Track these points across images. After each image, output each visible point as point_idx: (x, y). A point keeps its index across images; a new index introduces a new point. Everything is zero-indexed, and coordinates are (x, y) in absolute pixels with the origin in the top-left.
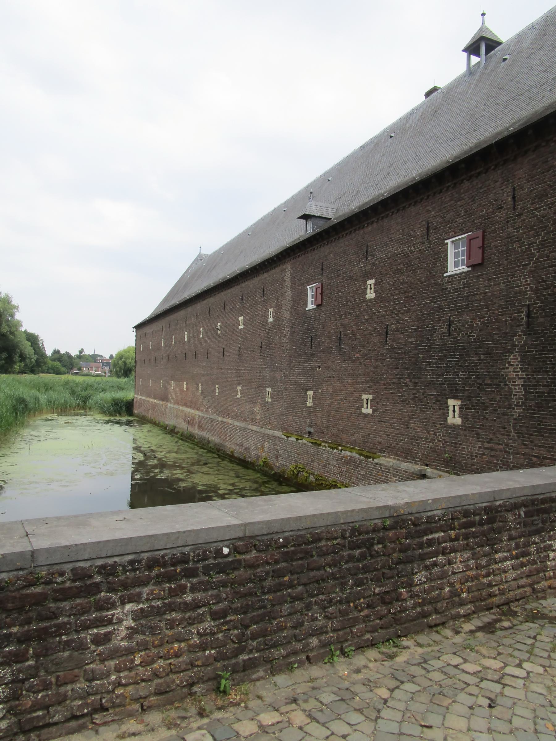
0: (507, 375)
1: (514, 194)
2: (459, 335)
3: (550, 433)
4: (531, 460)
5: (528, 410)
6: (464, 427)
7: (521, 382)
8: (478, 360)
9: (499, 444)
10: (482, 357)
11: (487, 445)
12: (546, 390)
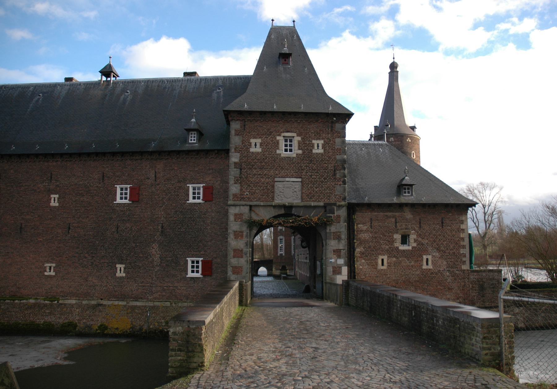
0: (151, 253)
1: (156, 175)
2: (123, 233)
3: (173, 276)
4: (163, 288)
5: (162, 267)
6: (127, 277)
7: (159, 256)
8: (135, 246)
9: (148, 283)
10: (138, 244)
11: (140, 285)
12: (170, 259)
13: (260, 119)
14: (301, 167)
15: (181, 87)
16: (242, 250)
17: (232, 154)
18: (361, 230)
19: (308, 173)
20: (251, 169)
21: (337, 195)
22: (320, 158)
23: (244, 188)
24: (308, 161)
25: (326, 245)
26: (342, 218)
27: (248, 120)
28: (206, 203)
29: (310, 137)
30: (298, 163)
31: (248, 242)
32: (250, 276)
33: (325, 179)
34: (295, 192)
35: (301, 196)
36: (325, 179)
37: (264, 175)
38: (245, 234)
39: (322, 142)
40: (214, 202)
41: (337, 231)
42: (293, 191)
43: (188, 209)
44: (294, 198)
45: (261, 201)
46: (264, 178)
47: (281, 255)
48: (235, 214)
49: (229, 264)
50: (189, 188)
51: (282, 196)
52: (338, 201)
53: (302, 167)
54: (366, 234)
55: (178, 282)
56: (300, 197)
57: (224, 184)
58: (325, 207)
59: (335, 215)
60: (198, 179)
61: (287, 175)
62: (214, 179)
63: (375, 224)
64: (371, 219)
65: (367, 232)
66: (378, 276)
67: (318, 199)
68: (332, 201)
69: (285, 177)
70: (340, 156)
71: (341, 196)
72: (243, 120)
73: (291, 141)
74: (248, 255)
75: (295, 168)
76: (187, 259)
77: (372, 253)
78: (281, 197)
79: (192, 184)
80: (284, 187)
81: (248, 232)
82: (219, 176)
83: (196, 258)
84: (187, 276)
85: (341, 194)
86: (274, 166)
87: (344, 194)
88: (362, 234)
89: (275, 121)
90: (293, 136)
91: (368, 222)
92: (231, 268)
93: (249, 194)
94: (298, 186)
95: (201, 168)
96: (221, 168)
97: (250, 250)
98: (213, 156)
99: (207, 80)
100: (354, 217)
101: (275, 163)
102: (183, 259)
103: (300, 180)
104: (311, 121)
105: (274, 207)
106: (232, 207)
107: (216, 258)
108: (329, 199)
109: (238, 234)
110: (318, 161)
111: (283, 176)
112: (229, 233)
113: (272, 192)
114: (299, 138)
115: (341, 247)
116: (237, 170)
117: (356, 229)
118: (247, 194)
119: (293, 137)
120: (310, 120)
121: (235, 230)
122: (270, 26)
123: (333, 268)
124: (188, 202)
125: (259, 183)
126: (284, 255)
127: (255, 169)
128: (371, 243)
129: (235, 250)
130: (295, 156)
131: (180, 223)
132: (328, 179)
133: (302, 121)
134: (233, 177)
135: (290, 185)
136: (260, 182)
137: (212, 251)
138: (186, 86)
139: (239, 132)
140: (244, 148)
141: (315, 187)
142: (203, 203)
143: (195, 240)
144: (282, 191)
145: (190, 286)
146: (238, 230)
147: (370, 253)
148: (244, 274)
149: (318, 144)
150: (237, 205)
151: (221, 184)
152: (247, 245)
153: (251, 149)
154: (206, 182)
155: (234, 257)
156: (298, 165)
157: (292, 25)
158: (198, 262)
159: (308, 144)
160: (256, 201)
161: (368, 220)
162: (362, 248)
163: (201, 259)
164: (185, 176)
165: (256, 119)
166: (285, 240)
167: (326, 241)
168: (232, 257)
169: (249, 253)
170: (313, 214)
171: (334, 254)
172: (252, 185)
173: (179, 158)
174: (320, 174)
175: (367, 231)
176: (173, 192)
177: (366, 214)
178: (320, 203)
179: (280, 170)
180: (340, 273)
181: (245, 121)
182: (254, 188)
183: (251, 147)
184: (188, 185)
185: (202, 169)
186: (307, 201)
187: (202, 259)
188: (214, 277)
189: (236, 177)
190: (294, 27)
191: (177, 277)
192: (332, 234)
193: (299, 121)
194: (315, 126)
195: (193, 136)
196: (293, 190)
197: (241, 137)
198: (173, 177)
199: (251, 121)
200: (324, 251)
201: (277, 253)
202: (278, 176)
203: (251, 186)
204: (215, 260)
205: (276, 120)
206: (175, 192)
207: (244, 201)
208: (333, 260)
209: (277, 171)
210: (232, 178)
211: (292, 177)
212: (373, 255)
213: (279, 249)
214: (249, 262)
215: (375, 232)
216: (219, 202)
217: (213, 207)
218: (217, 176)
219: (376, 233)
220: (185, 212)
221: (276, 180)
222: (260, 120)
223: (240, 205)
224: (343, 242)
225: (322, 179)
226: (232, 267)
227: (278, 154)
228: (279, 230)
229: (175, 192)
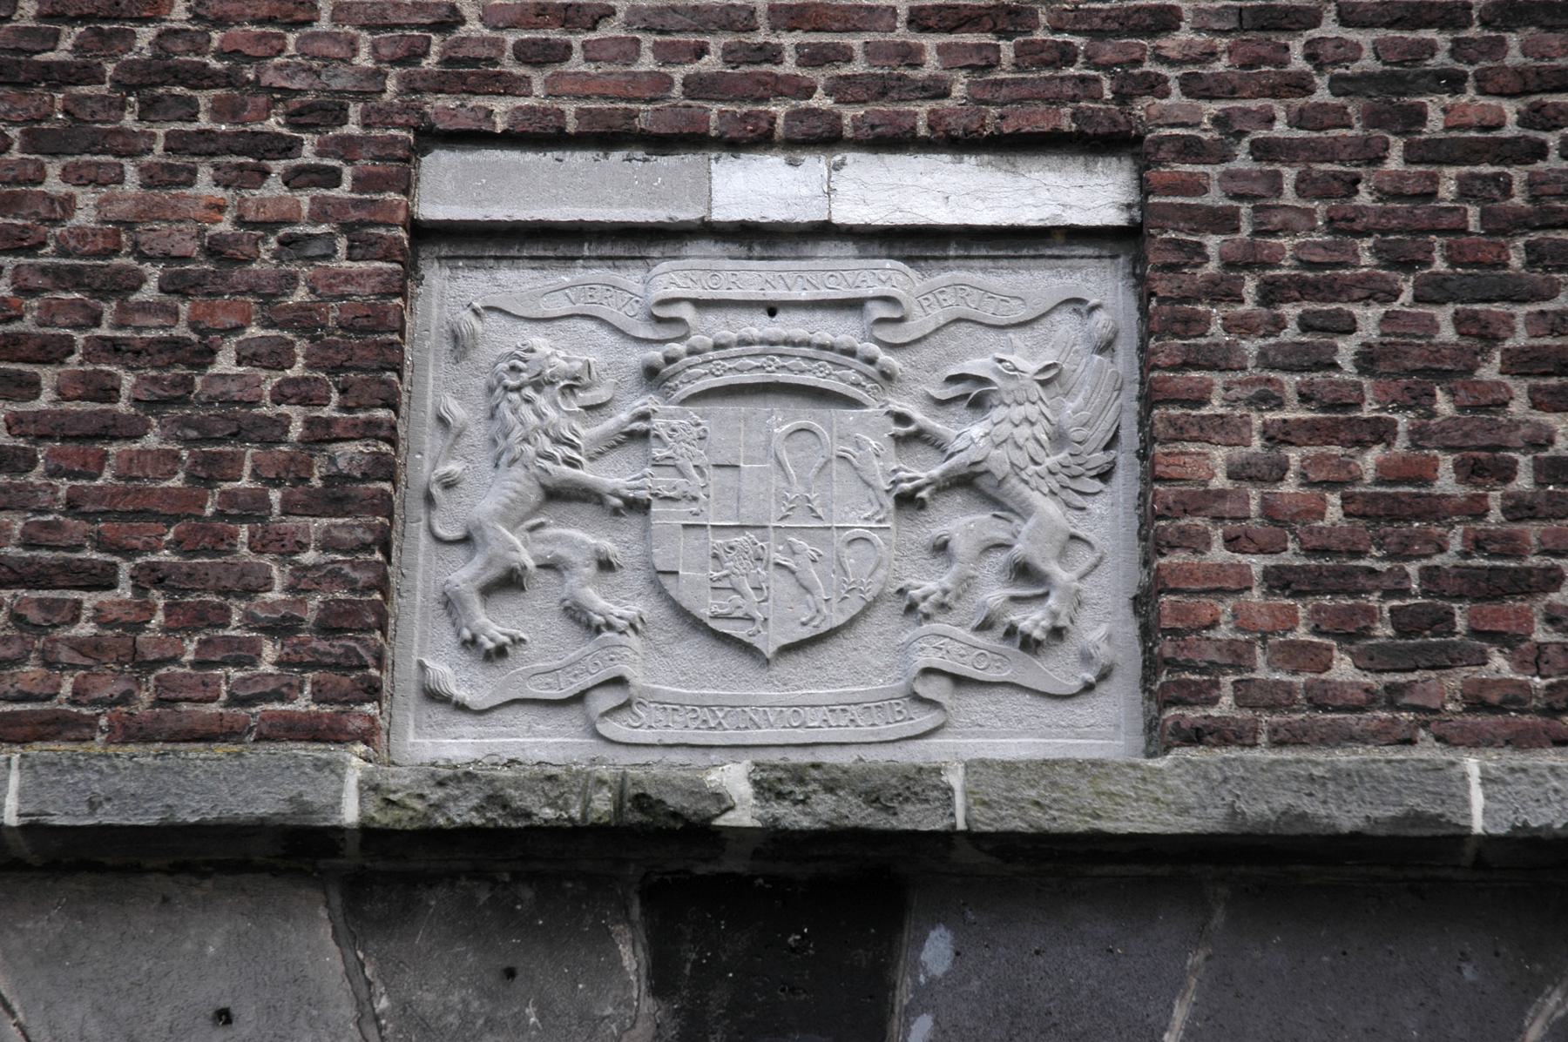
35: (1142, 602)
42: (924, 469)
46: (130, 147)
51: (599, 600)
69: (692, 140)
78: (579, 617)
80: (652, 376)
111: (646, 116)
113: (336, 497)
141: (1518, 364)
144: (614, 476)
196: (912, 438)
202: (502, 111)
221: (431, 209)
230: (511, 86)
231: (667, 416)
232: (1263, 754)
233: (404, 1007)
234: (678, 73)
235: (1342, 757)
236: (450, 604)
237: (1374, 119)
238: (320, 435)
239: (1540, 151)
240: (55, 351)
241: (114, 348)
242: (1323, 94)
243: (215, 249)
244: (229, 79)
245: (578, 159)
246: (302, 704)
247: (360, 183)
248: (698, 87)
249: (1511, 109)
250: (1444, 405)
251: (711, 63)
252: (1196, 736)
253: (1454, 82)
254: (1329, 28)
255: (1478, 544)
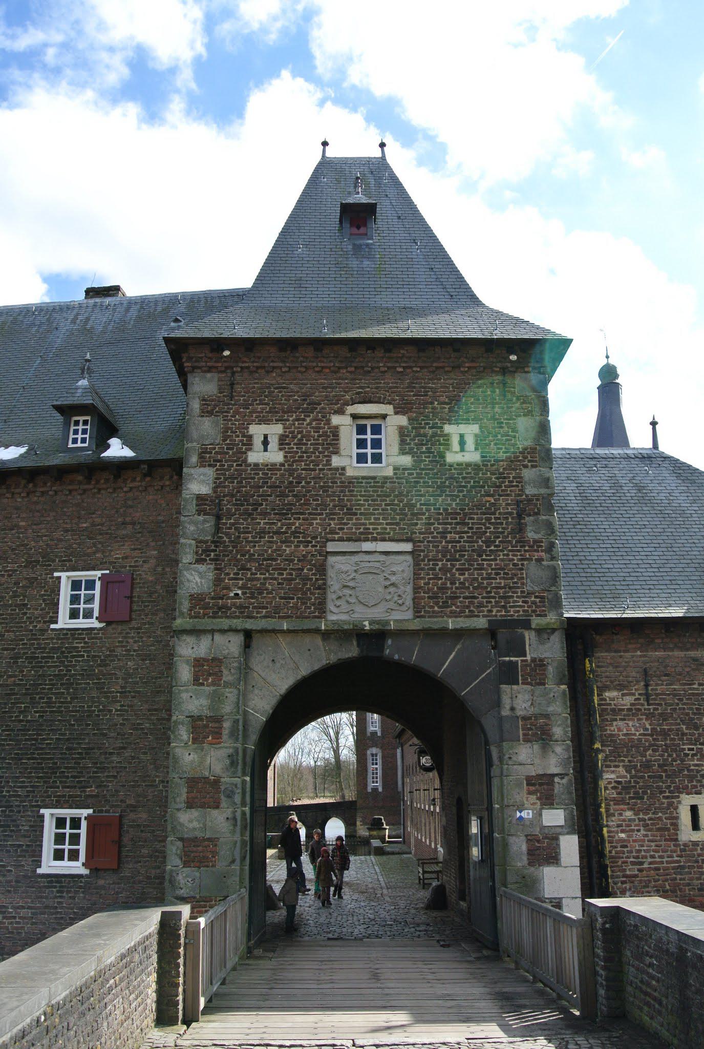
13: (281, 364)
14: (411, 506)
15: (74, 321)
16: (217, 782)
17: (192, 471)
18: (613, 710)
19: (433, 524)
20: (250, 514)
21: (530, 594)
22: (472, 478)
23: (228, 574)
24: (431, 489)
25: (501, 759)
26: (550, 668)
27: (242, 368)
28: (110, 628)
29: (435, 415)
30: (401, 494)
31: (237, 753)
32: (242, 870)
33: (488, 543)
34: (393, 584)
35: (414, 599)
36: (488, 543)
37: (293, 533)
38: (227, 725)
39: (475, 428)
40: (134, 624)
41: (536, 710)
42: (388, 583)
43: (53, 648)
44: (391, 605)
45: (283, 617)
46: (293, 542)
47: (375, 790)
48: (195, 659)
49: (174, 828)
50: (60, 582)
51: (350, 600)
52: (534, 611)
53: (414, 505)
54: (631, 723)
55: (9, 891)
56: (409, 602)
57: (168, 569)
58: (492, 632)
59: (528, 658)
60: (88, 555)
61: (367, 532)
62: (136, 554)
63: (660, 687)
64: (645, 671)
65: (633, 715)
66: (682, 867)
67: (468, 607)
68: (515, 613)
70: (534, 469)
71: (543, 597)
72: (227, 368)
73: (377, 430)
74: (238, 799)
75: (391, 509)
76: (42, 811)
77: (658, 787)
78: (348, 602)
79: (67, 571)
81: (238, 720)
82: (153, 544)
83: (71, 807)
84: (39, 871)
85: (544, 591)
86: (324, 505)
87: (553, 588)
88: (620, 723)
89: (328, 370)
90: (383, 412)
91: (638, 682)
92: (180, 844)
93: (244, 593)
94: (403, 568)
95: (98, 520)
96: (161, 518)
97: (244, 782)
98: (137, 484)
99: (144, 302)
100: (588, 665)
101: (328, 496)
102: (29, 813)
103: (408, 547)
104: (437, 368)
105: (326, 635)
106: (185, 637)
107: (133, 808)
108: (504, 607)
109: (206, 726)
110: (464, 487)
112: (175, 722)
113: (319, 588)
114: (403, 420)
115: (553, 765)
116: (205, 521)
117: (599, 705)
118: (237, 595)
119: (384, 417)
120: (435, 365)
121: (196, 713)
122: (318, 158)
123: (528, 841)
124: (53, 626)
125: (276, 560)
126: (380, 789)
127: (264, 514)
128: (650, 752)
129: (193, 783)
130: (389, 472)
131: (26, 694)
132: (497, 543)
133: (411, 367)
134: (193, 542)
135: (377, 565)
136: (280, 555)
137: (124, 786)
138: (88, 319)
139: (215, 406)
140: (231, 452)
141: (458, 570)
142: (101, 629)
143: (68, 749)
144: (351, 584)
145: (47, 907)
146: (207, 712)
147: (651, 787)
148: (221, 865)
149: (462, 436)
150: (204, 632)
151: (160, 569)
152: (233, 763)
153: (249, 453)
154: (111, 563)
155: (190, 805)
156: (401, 501)
157: (379, 155)
158: (76, 823)
159: (433, 436)
160: (265, 617)
161: (634, 674)
162: (621, 770)
163: (85, 812)
164: (47, 545)
165: (266, 365)
166: (383, 757)
167: (500, 748)
168: (183, 805)
169: (239, 791)
170: (454, 657)
171: (530, 793)
172: (253, 566)
173: (34, 492)
174: (472, 528)
175: (633, 712)
176: (11, 597)
177: (628, 655)
178: (475, 619)
179: (343, 519)
180: (553, 858)
181: (233, 373)
182: (258, 576)
183: (250, 449)
184: (56, 574)
185: (102, 525)
186: (434, 615)
187: (90, 811)
188: (126, 873)
189: (201, 542)
190: (383, 157)
191: (4, 876)
192: (521, 723)
193: (401, 370)
194: (451, 381)
195: (81, 427)
196: (387, 579)
197: (220, 420)
198: (13, 550)
199: (251, 372)
200: (495, 782)
201: (366, 785)
202: (336, 536)
203: (249, 569)
204: (132, 816)
205: (329, 368)
206: (15, 595)
207: (227, 617)
208: (527, 814)
209: (333, 519)
210: (190, 545)
211: (383, 540)
212: (661, 792)
213: (370, 776)
214: (239, 823)
215: (661, 715)
216: (149, 623)
217: (131, 641)
218: (148, 544)
219: (664, 717)
220: (43, 658)
222: (280, 368)
223: (212, 632)
224: (559, 749)
225: (480, 543)
226: (181, 839)
227: (337, 469)
228: (369, 734)
229: (15, 595)
230: (338, 533)
231: (358, 576)
232: (427, 619)
233: (329, 649)
234: (358, 531)
235: (435, 620)
236: (333, 600)
237: (441, 537)
238: (317, 580)
239: (460, 542)
240: (286, 569)
241: (292, 569)
242: (435, 534)
243: (303, 556)
244: (303, 533)
245: (346, 543)
246: (317, 614)
247: (320, 547)
248: (361, 533)
249: (457, 536)
250: (448, 575)
251: (362, 530)
252: (418, 617)
253: (451, 533)
254: (436, 525)
255: (451, 593)
